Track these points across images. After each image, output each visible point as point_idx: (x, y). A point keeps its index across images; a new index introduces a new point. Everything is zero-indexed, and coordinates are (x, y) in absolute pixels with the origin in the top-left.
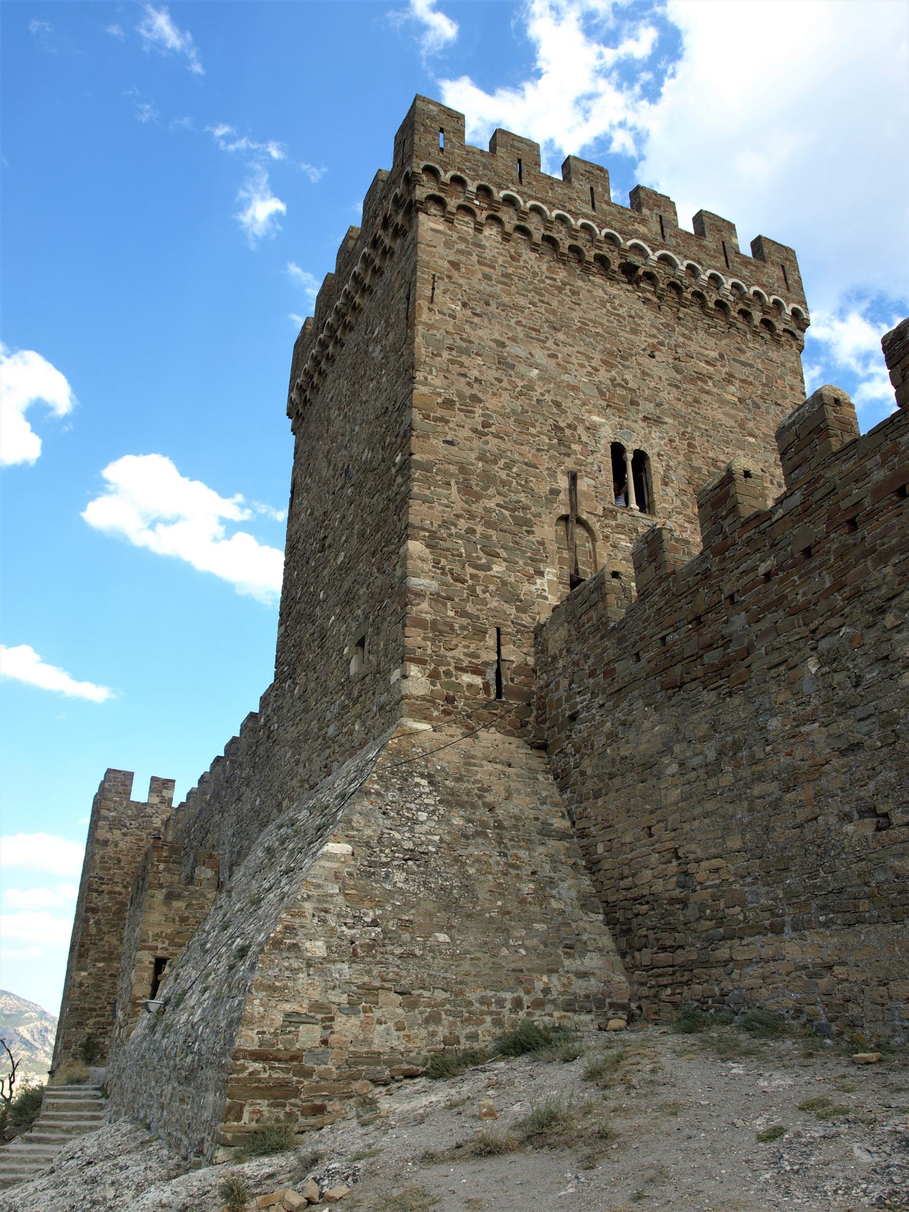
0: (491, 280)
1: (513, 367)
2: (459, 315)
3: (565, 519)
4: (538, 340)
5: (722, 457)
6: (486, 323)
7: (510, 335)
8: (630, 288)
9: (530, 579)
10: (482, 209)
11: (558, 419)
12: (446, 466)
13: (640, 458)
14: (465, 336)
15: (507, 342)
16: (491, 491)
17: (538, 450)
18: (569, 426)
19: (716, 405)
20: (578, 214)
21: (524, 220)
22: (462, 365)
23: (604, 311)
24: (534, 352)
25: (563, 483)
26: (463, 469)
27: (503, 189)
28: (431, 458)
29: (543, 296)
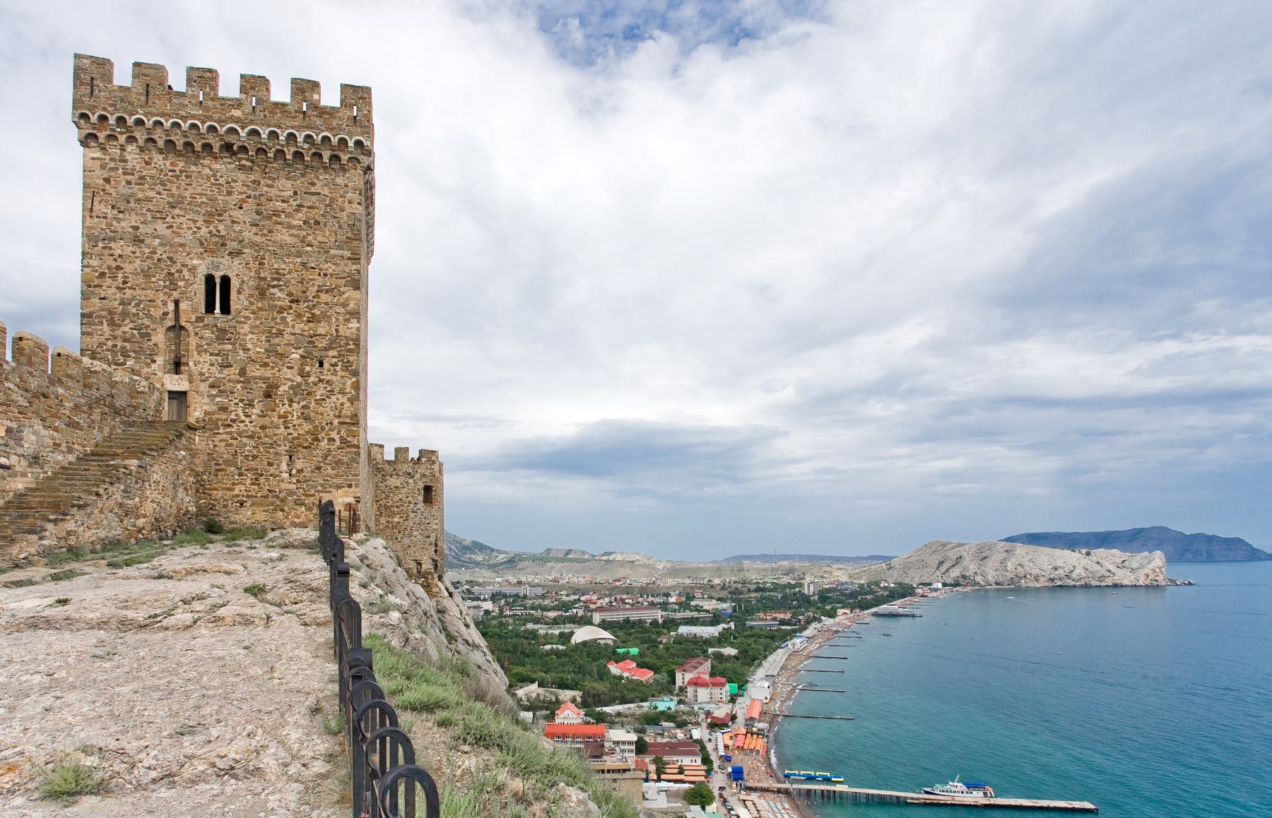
1: (143, 241)
2: (109, 216)
4: (160, 218)
5: (283, 266)
6: (127, 216)
7: (142, 220)
8: (229, 160)
9: (148, 365)
10: (121, 133)
13: (226, 281)
14: (113, 228)
15: (140, 226)
17: (157, 291)
19: (284, 231)
21: (151, 133)
22: (110, 248)
23: (209, 184)
24: (157, 228)
25: (171, 307)
26: (110, 313)
27: (133, 115)
29: (166, 185)
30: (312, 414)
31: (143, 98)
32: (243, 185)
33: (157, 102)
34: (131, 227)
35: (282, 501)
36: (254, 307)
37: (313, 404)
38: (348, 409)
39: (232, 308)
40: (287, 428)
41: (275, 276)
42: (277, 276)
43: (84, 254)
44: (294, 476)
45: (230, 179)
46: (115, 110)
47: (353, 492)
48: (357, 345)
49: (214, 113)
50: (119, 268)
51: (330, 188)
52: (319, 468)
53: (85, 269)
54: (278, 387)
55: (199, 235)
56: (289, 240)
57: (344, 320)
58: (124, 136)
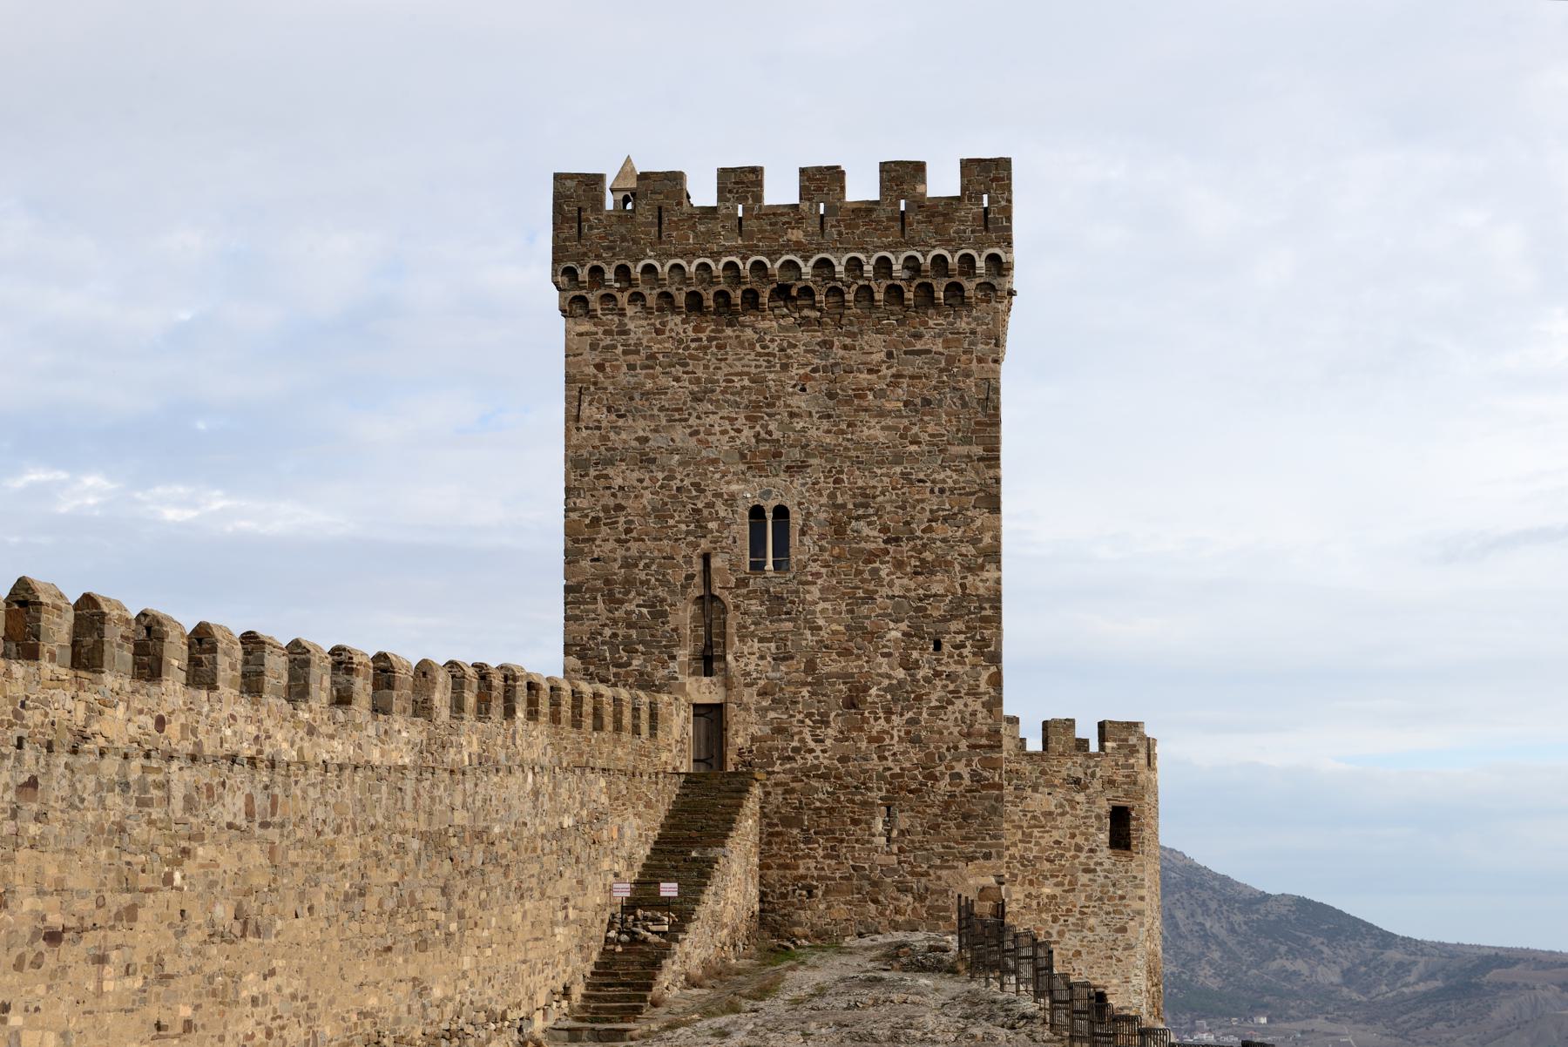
0: (635, 369)
1: (653, 461)
3: (701, 597)
5: (872, 483)
6: (630, 422)
10: (621, 290)
12: (594, 582)
13: (781, 513)
14: (610, 444)
16: (633, 594)
17: (676, 540)
19: (873, 422)
20: (719, 253)
22: (606, 477)
23: (753, 354)
25: (698, 566)
26: (607, 582)
27: (640, 260)
28: (580, 579)
29: (688, 365)
30: (924, 733)
31: (654, 230)
32: (806, 351)
33: (674, 234)
34: (637, 439)
35: (874, 884)
36: (826, 556)
37: (925, 715)
38: (983, 723)
39: (793, 559)
40: (882, 758)
41: (860, 500)
42: (863, 500)
43: (568, 490)
44: (894, 842)
45: (785, 344)
46: (614, 255)
47: (993, 868)
48: (997, 608)
49: (759, 240)
50: (619, 508)
51: (946, 341)
52: (936, 827)
53: (571, 514)
54: (866, 689)
55: (738, 442)
56: (882, 436)
58: (626, 294)
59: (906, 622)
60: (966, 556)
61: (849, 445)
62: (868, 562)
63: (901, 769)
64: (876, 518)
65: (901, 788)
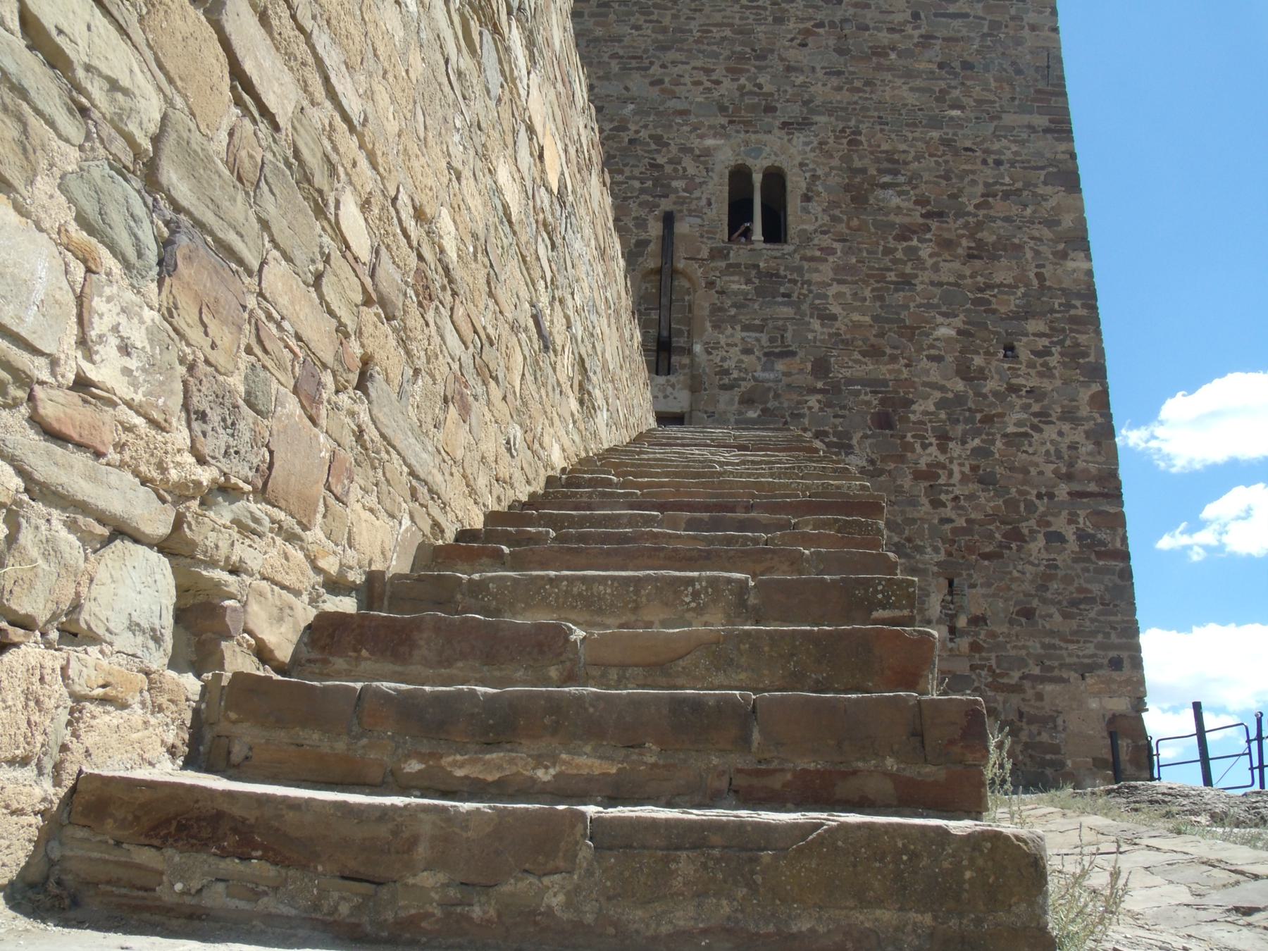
3: (659, 271)
4: (638, 69)
5: (903, 147)
7: (601, 73)
11: (655, 156)
13: (775, 179)
18: (670, 162)
19: (899, 82)
24: (630, 85)
37: (999, 444)
38: (1087, 462)
40: (937, 504)
41: (886, 165)
42: (890, 166)
44: (963, 633)
48: (1093, 308)
54: (908, 403)
55: (716, 94)
56: (911, 99)
57: (1055, 254)
59: (962, 316)
60: (1040, 240)
61: (867, 104)
62: (902, 237)
63: (968, 521)
64: (909, 188)
65: (971, 550)
